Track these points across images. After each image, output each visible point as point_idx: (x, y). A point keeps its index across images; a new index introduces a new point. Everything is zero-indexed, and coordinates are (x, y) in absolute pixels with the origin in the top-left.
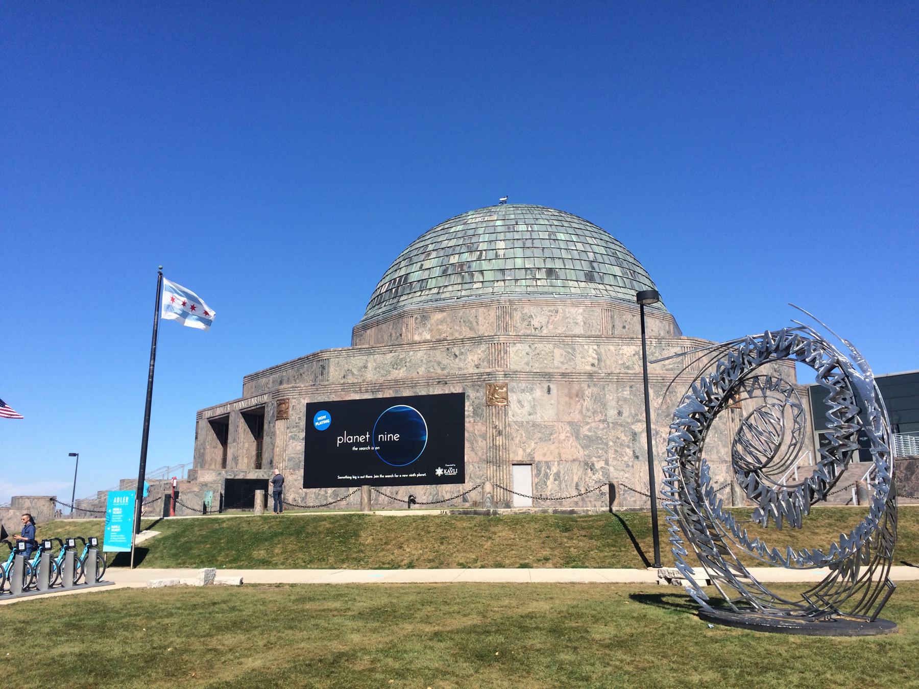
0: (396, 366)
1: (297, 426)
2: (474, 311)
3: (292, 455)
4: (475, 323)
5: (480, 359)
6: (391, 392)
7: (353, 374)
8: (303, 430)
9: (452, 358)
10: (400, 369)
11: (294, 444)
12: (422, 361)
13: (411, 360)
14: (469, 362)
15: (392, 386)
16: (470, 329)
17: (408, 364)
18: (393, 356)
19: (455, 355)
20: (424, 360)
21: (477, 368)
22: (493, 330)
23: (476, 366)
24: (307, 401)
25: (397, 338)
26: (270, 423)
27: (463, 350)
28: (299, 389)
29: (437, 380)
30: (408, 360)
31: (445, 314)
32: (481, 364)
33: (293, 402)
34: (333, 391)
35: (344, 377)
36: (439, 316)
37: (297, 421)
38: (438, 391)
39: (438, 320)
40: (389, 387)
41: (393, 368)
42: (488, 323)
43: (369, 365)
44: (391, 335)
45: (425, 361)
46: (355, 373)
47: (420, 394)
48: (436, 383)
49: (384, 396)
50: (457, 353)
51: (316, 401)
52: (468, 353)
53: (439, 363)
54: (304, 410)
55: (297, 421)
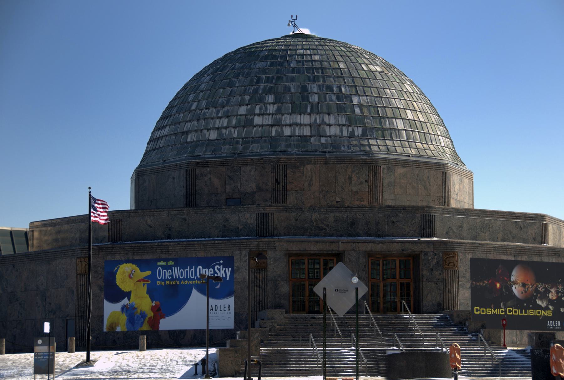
0: (483, 230)
1: (464, 277)
2: (427, 171)
3: (462, 301)
4: (427, 183)
5: (536, 234)
6: (526, 257)
7: (453, 231)
8: (469, 280)
9: (519, 230)
10: (485, 233)
11: (463, 291)
12: (500, 228)
13: (492, 227)
14: (529, 235)
15: (527, 253)
16: (424, 188)
17: (491, 230)
18: (481, 221)
19: (520, 227)
20: (501, 228)
21: (535, 240)
22: (440, 192)
23: (533, 238)
24: (470, 257)
25: (361, 183)
26: (432, 270)
27: (525, 224)
28: (464, 245)
29: (554, 252)
30: (491, 226)
31: (405, 169)
32: (537, 237)
33: (461, 256)
34: (488, 251)
35: (447, 233)
36: (400, 170)
37: (464, 272)
38: (554, 260)
39: (400, 174)
40: (525, 253)
41: (481, 231)
42: (437, 185)
43: (465, 225)
44: (350, 178)
45: (501, 229)
46: (455, 231)
47: (544, 261)
48: (553, 254)
49: (522, 260)
50: (522, 227)
51: (476, 257)
52: (529, 227)
53: (511, 233)
54: (468, 263)
55: (464, 272)
